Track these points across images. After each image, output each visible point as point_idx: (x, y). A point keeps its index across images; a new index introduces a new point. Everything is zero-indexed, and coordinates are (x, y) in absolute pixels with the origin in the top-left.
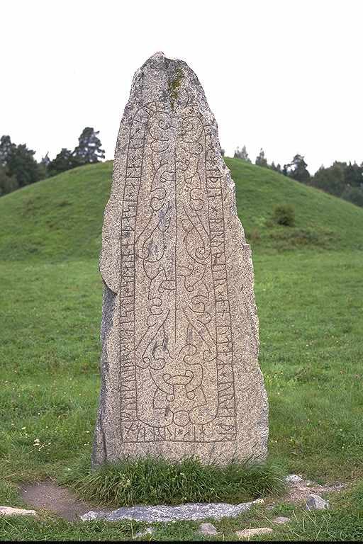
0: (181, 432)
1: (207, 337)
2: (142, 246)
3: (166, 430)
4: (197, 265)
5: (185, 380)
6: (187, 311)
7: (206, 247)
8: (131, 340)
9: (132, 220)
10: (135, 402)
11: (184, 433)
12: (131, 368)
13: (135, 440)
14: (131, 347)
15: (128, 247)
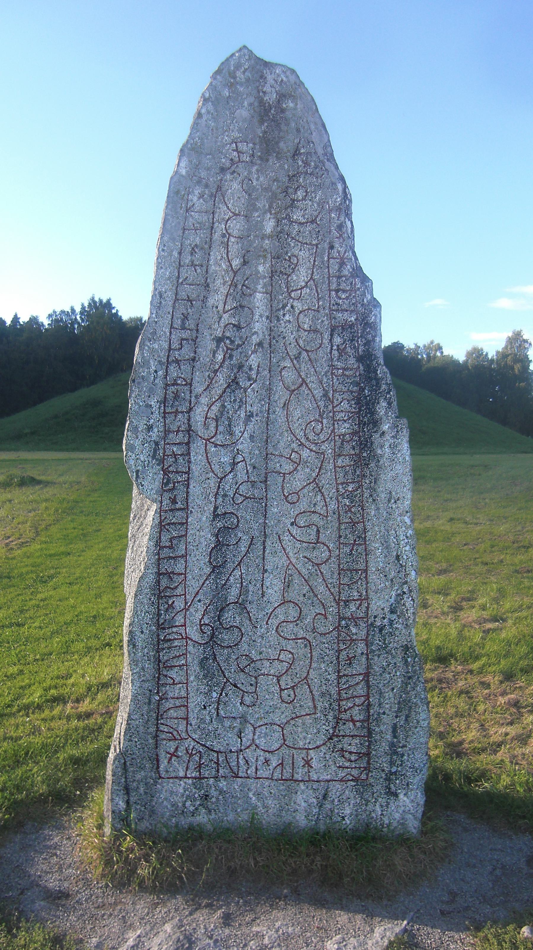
0: (267, 761)
1: (321, 589)
2: (203, 414)
3: (241, 757)
4: (305, 453)
5: (279, 667)
6: (286, 538)
7: (325, 421)
8: (179, 591)
9: (186, 367)
10: (184, 706)
11: (274, 763)
12: (176, 643)
13: (182, 774)
14: (179, 604)
15: (180, 416)
